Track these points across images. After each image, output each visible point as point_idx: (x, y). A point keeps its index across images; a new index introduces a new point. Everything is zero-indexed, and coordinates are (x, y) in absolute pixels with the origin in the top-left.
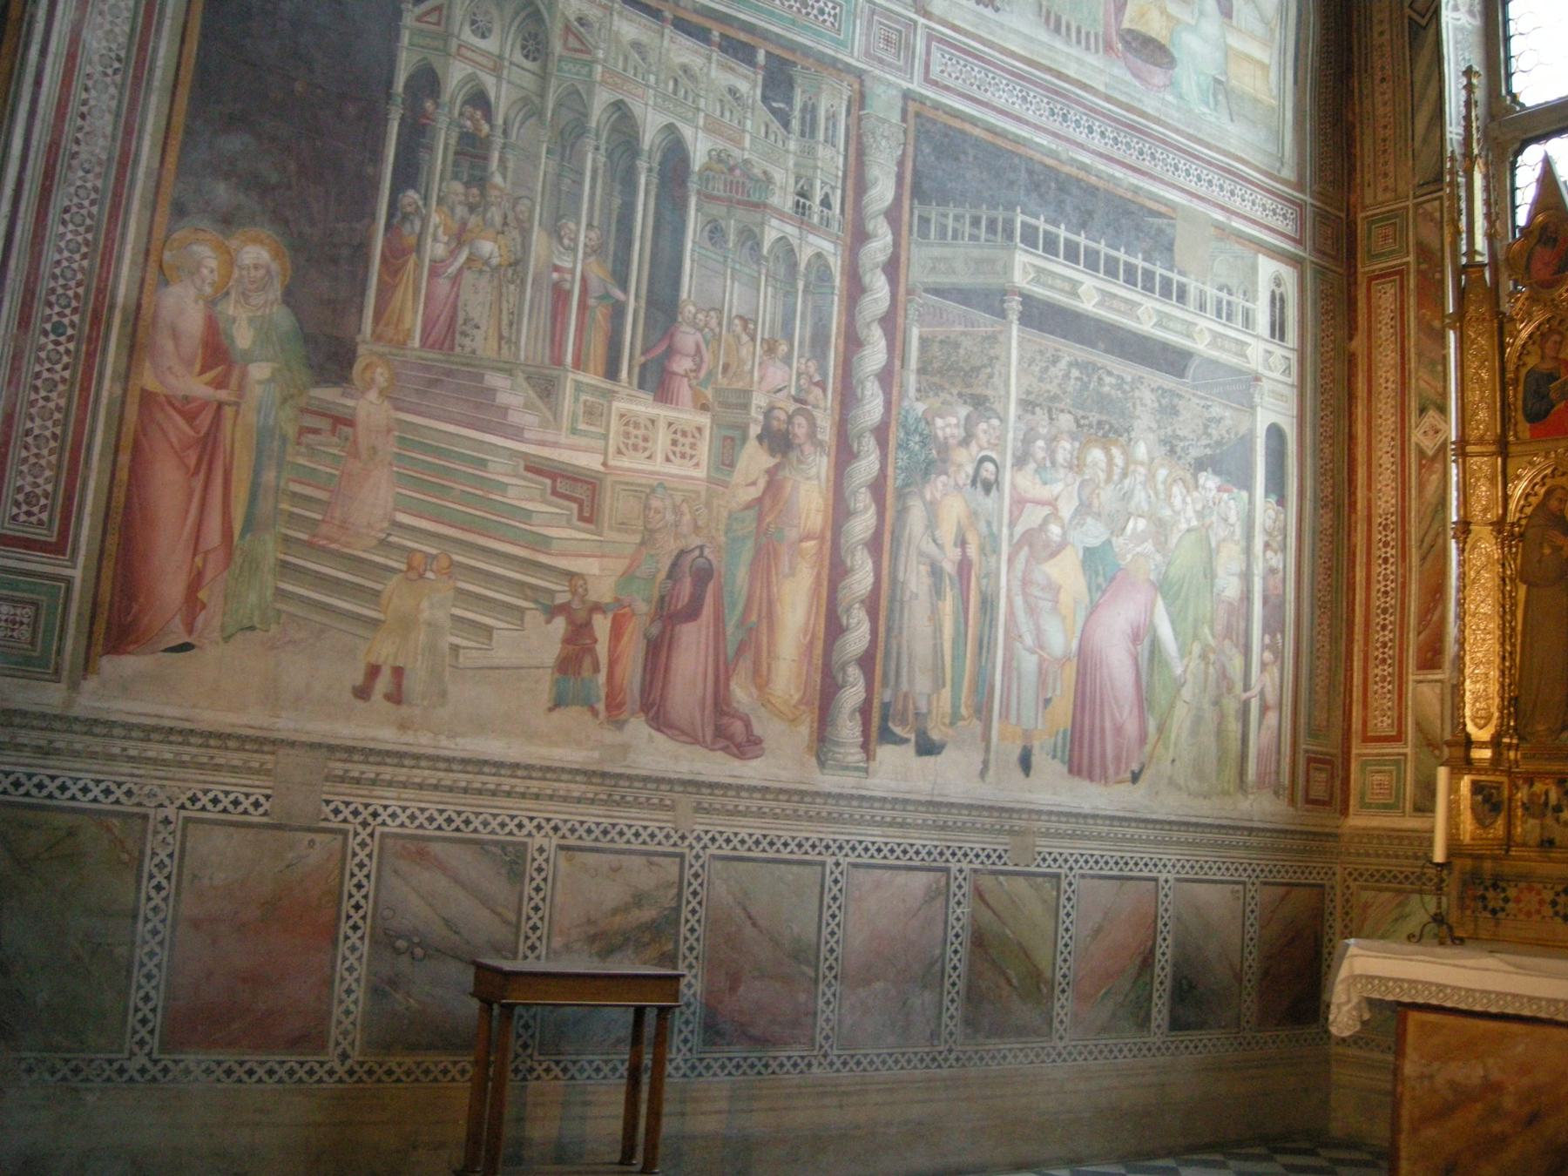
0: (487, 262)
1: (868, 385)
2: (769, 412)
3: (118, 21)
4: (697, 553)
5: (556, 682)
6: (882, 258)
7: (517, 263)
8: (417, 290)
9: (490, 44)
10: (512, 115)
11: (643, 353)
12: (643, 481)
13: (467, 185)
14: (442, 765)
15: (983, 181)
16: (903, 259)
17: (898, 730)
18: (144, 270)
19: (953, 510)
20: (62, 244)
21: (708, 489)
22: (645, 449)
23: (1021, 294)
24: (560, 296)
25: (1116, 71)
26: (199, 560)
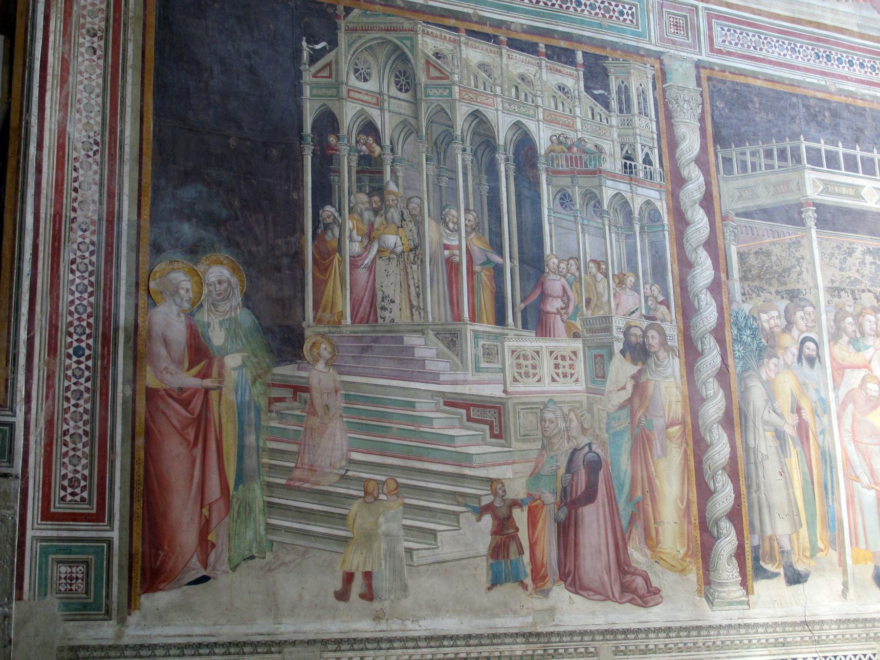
0: (392, 252)
1: (703, 297)
2: (626, 333)
3: (92, 115)
4: (587, 449)
5: (491, 566)
6: (698, 196)
7: (416, 248)
9: (371, 85)
10: (396, 137)
11: (522, 302)
12: (538, 400)
13: (370, 195)
14: (410, 644)
15: (770, 121)
16: (715, 194)
17: (769, 567)
18: (137, 298)
19: (786, 384)
20: (73, 288)
21: (588, 398)
22: (535, 375)
23: (814, 205)
24: (452, 267)
25: (865, 13)
26: (205, 511)
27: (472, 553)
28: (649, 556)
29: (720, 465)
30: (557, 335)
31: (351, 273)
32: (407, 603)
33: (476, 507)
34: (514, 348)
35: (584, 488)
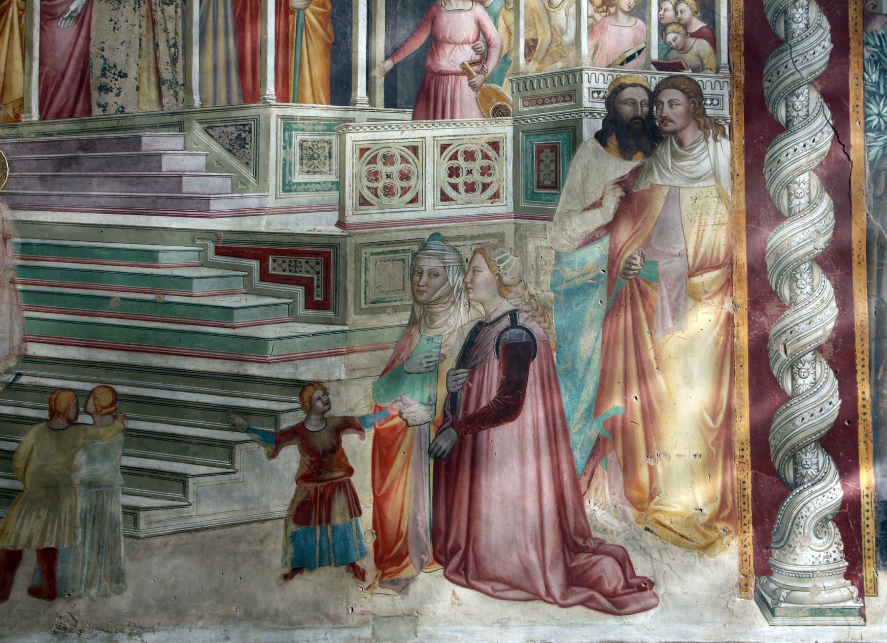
2: (613, 98)
4: (506, 322)
5: (293, 538)
8: (26, 46)
11: (387, 58)
12: (408, 236)
21: (517, 228)
22: (405, 191)
27: (256, 515)
28: (633, 519)
29: (809, 343)
30: (458, 114)
31: (42, 29)
32: (121, 602)
33: (269, 432)
34: (364, 145)
35: (494, 394)
